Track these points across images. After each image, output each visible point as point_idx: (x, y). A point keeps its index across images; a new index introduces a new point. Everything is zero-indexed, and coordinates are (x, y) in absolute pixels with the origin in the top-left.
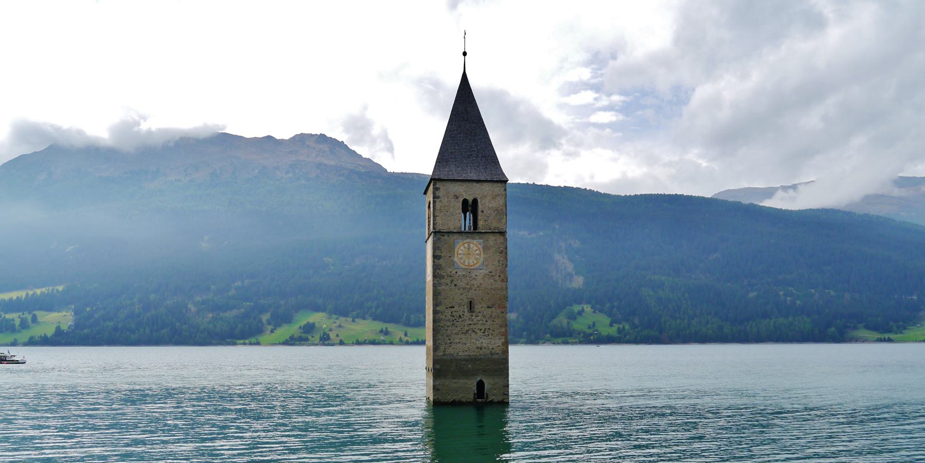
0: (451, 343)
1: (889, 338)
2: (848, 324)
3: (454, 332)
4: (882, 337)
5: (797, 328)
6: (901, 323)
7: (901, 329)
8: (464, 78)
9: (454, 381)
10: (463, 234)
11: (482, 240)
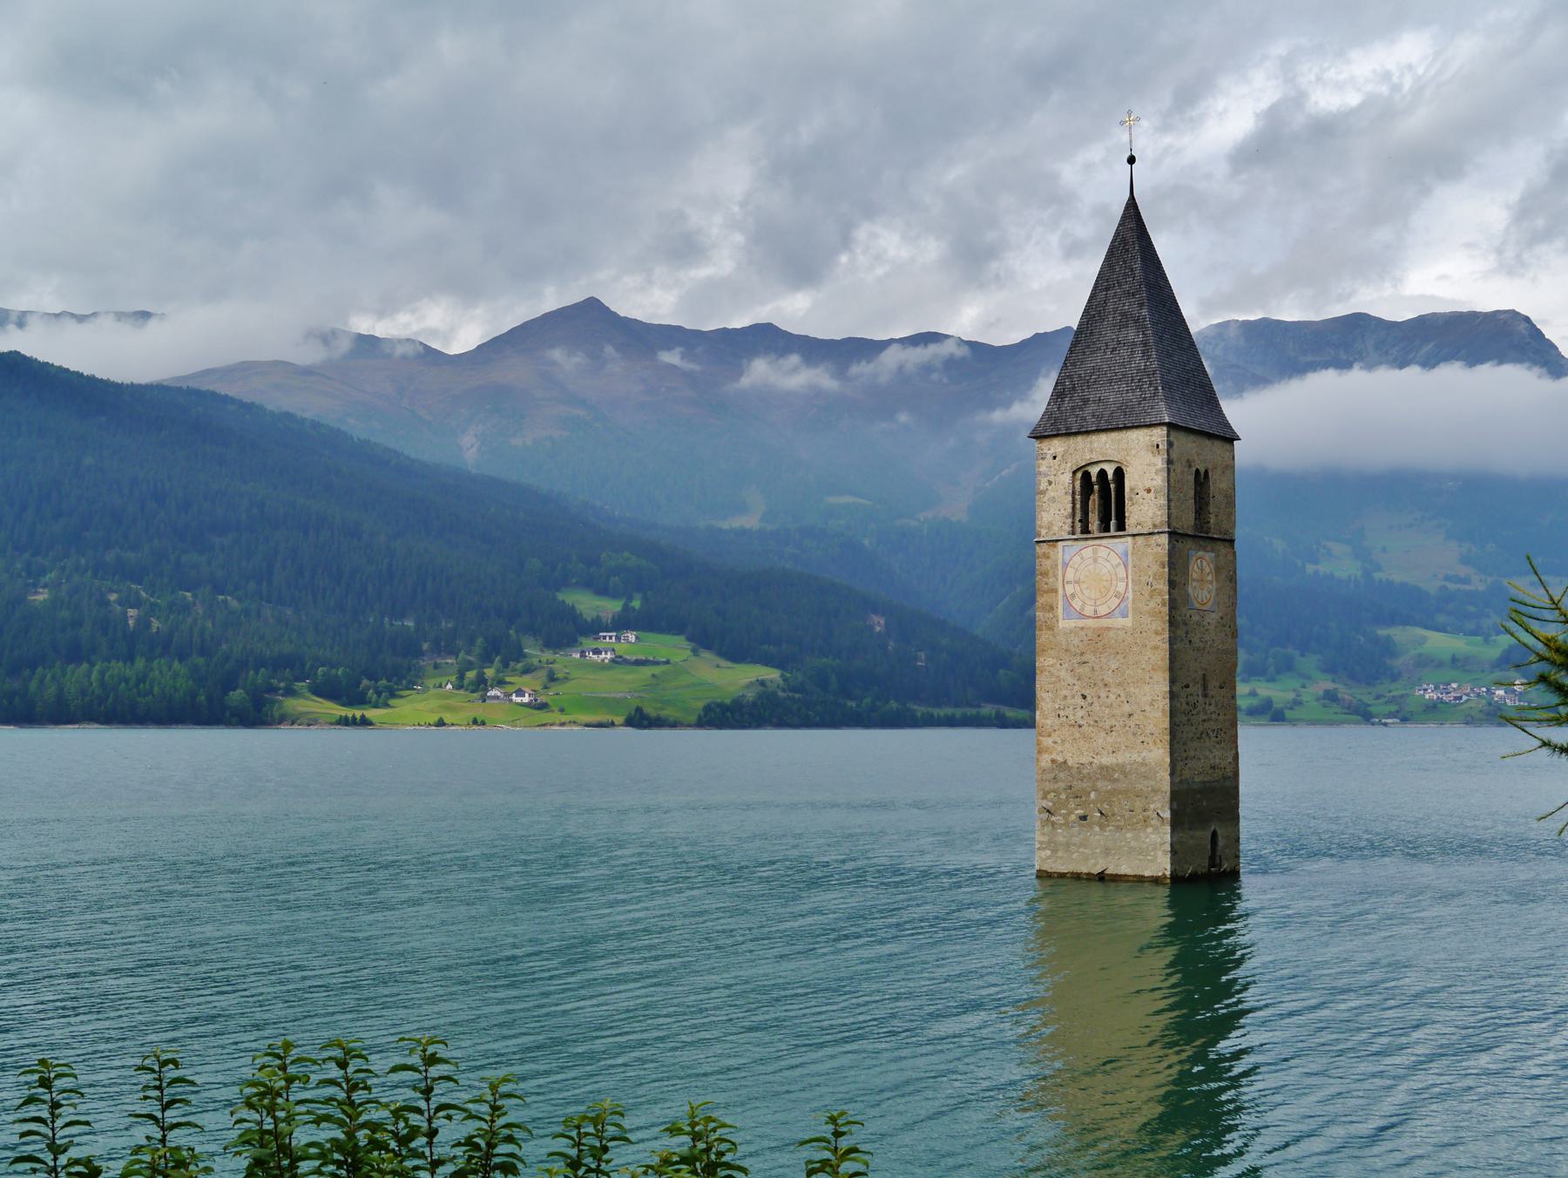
0: (1186, 759)
1: (363, 716)
2: (274, 682)
3: (1191, 735)
4: (350, 715)
5: (156, 689)
6: (384, 682)
7: (386, 697)
8: (1132, 207)
9: (1191, 833)
10: (1197, 540)
11: (1213, 555)
